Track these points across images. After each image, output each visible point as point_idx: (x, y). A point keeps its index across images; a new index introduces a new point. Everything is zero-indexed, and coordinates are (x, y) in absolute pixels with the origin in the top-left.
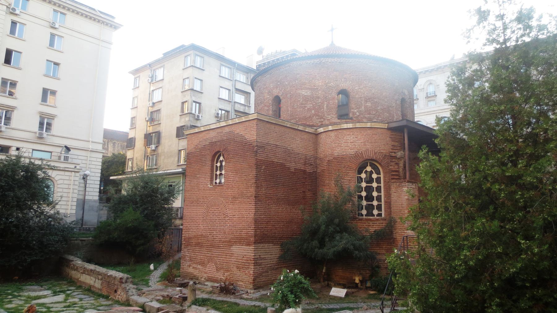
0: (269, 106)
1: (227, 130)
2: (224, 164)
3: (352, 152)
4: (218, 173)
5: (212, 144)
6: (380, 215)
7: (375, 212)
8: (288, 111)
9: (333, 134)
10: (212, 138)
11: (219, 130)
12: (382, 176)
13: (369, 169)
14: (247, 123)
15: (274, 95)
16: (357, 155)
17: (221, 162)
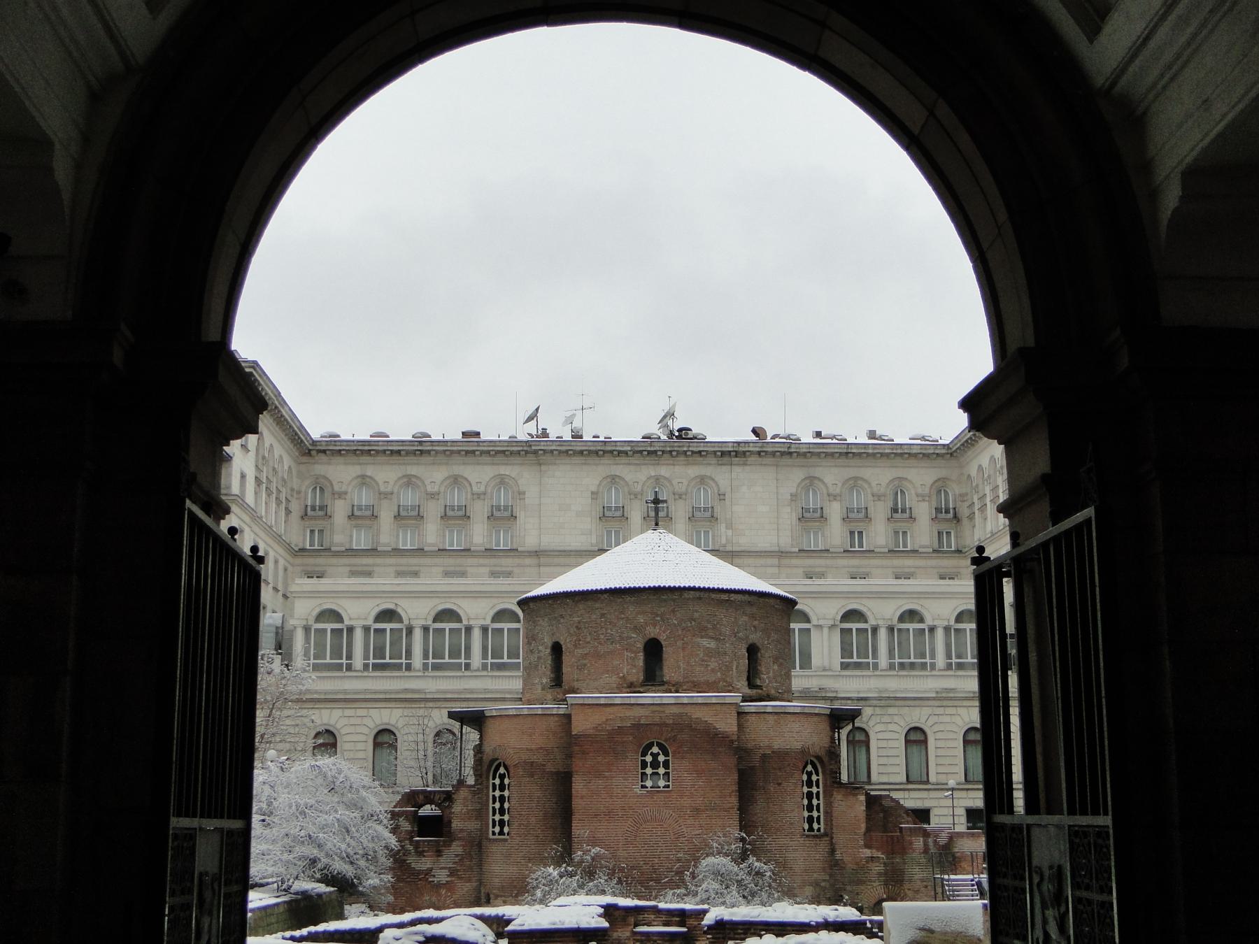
0: (636, 653)
1: (675, 710)
2: (661, 758)
3: (798, 745)
4: (649, 771)
5: (637, 726)
6: (819, 830)
7: (815, 826)
8: (679, 667)
9: (771, 718)
10: (640, 718)
11: (655, 708)
12: (820, 778)
13: (809, 768)
14: (718, 707)
15: (649, 637)
16: (804, 752)
17: (655, 756)
